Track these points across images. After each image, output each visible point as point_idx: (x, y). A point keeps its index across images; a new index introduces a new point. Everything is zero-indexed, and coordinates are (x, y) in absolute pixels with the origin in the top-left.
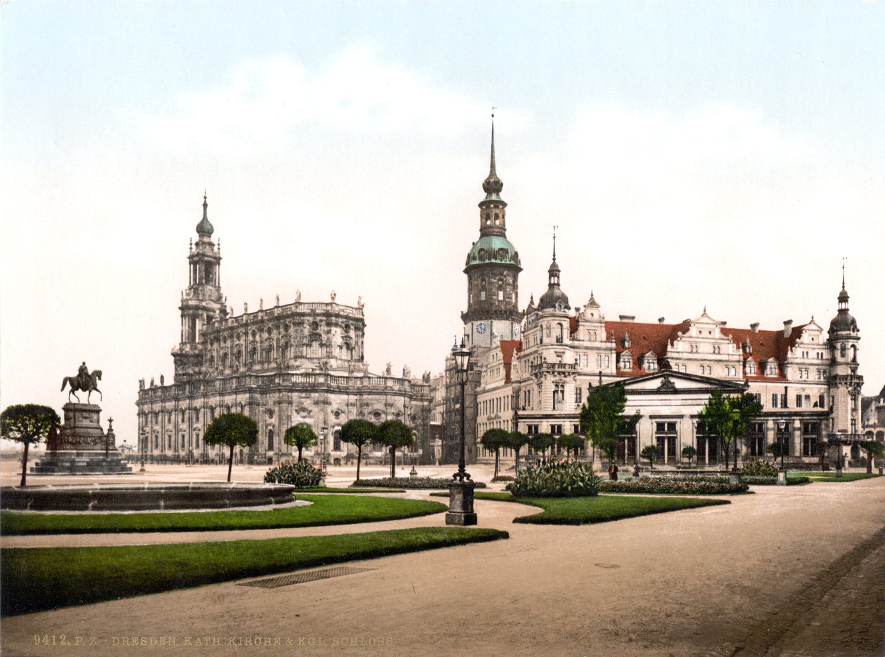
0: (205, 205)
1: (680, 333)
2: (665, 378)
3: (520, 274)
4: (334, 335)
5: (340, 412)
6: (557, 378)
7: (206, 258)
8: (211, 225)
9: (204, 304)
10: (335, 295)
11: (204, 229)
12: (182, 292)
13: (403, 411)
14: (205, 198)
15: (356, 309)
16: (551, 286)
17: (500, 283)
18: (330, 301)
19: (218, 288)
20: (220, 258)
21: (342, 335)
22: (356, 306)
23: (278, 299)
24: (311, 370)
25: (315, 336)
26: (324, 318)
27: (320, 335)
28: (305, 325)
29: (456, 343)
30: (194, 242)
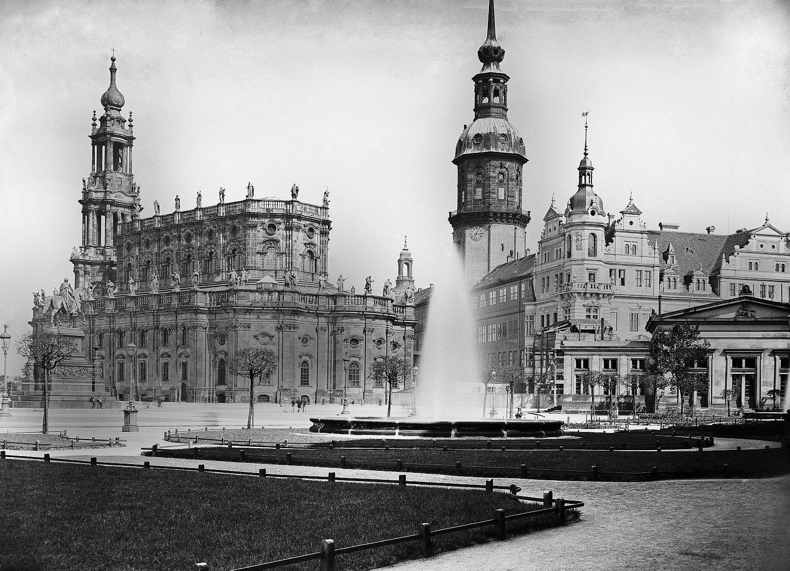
1: (737, 247)
2: (743, 306)
5: (308, 338)
6: (588, 302)
7: (114, 139)
8: (121, 95)
9: (112, 197)
10: (297, 191)
14: (113, 60)
15: (321, 208)
16: (582, 186)
17: (501, 177)
18: (290, 198)
20: (131, 139)
21: (306, 242)
22: (321, 204)
23: (222, 193)
27: (278, 241)
28: (259, 228)
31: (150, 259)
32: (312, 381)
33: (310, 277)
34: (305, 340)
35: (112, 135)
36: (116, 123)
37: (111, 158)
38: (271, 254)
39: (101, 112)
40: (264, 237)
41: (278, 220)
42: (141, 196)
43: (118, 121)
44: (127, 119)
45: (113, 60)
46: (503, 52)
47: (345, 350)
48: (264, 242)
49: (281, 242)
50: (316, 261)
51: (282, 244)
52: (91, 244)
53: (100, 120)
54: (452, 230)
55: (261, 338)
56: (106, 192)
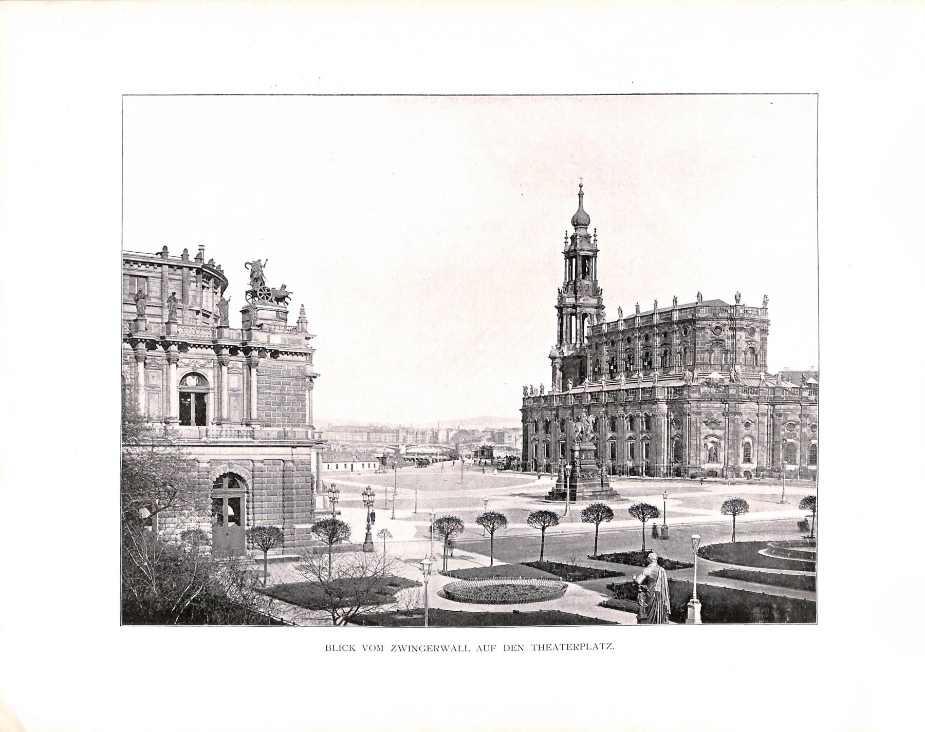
5: (750, 422)
7: (582, 253)
10: (740, 296)
14: (581, 186)
18: (733, 303)
19: (595, 282)
21: (747, 340)
23: (675, 300)
26: (726, 322)
28: (707, 330)
30: (569, 236)
34: (747, 425)
37: (580, 269)
39: (571, 231)
41: (723, 322)
44: (592, 234)
45: (581, 186)
47: (782, 433)
49: (726, 341)
50: (756, 356)
51: (728, 343)
53: (571, 238)
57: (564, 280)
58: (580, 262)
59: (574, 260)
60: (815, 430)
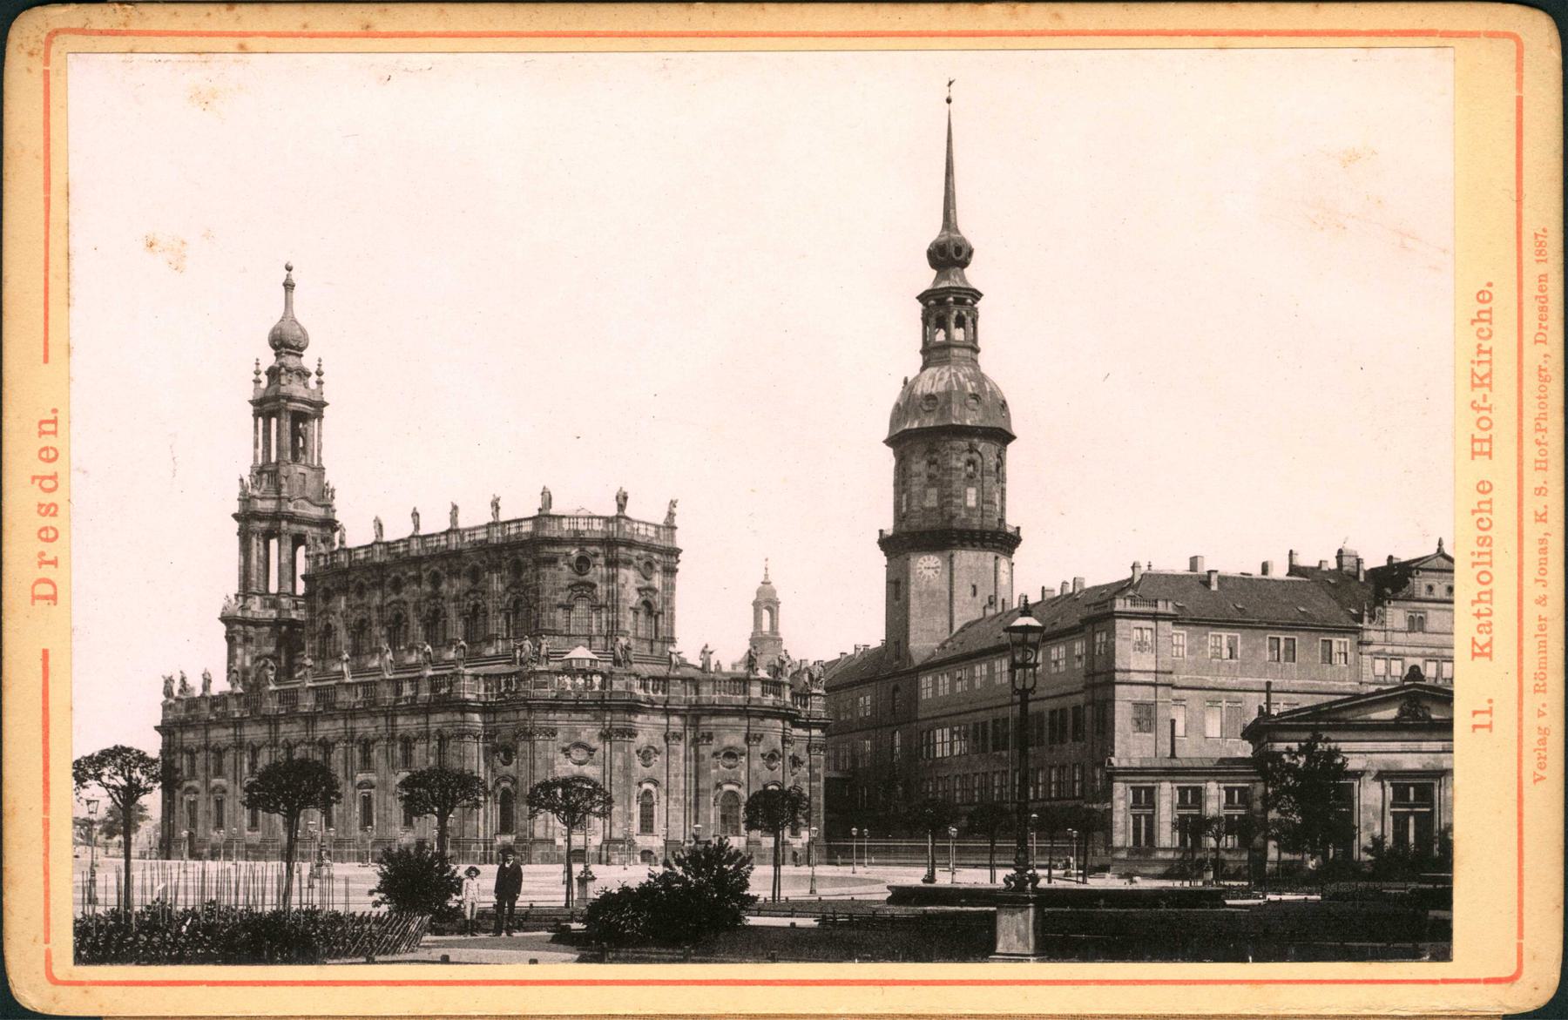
0: (289, 286)
3: (1010, 447)
4: (623, 586)
7: (293, 406)
9: (291, 507)
10: (625, 498)
11: (285, 343)
12: (242, 480)
13: (781, 751)
21: (640, 586)
23: (495, 505)
24: (587, 663)
25: (583, 589)
26: (598, 550)
27: (594, 586)
28: (561, 564)
29: (766, 576)
31: (365, 617)
32: (659, 826)
33: (646, 646)
35: (290, 398)
36: (295, 378)
37: (287, 439)
38: (581, 608)
39: (269, 359)
40: (569, 579)
42: (337, 503)
43: (299, 374)
44: (312, 369)
46: (971, 253)
48: (570, 587)
49: (599, 588)
50: (656, 618)
51: (601, 590)
52: (254, 589)
54: (884, 560)
55: (574, 752)
56: (280, 499)
57: (251, 462)
58: (287, 425)
59: (274, 421)
60: (774, 764)
